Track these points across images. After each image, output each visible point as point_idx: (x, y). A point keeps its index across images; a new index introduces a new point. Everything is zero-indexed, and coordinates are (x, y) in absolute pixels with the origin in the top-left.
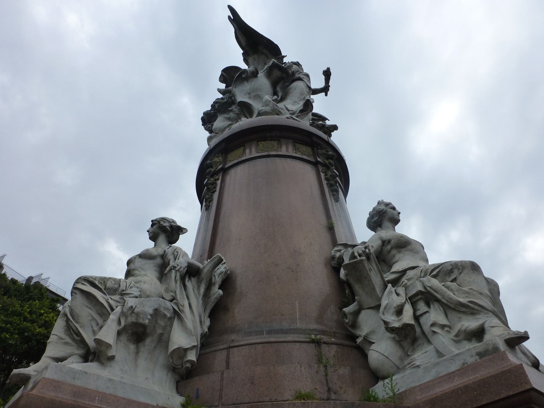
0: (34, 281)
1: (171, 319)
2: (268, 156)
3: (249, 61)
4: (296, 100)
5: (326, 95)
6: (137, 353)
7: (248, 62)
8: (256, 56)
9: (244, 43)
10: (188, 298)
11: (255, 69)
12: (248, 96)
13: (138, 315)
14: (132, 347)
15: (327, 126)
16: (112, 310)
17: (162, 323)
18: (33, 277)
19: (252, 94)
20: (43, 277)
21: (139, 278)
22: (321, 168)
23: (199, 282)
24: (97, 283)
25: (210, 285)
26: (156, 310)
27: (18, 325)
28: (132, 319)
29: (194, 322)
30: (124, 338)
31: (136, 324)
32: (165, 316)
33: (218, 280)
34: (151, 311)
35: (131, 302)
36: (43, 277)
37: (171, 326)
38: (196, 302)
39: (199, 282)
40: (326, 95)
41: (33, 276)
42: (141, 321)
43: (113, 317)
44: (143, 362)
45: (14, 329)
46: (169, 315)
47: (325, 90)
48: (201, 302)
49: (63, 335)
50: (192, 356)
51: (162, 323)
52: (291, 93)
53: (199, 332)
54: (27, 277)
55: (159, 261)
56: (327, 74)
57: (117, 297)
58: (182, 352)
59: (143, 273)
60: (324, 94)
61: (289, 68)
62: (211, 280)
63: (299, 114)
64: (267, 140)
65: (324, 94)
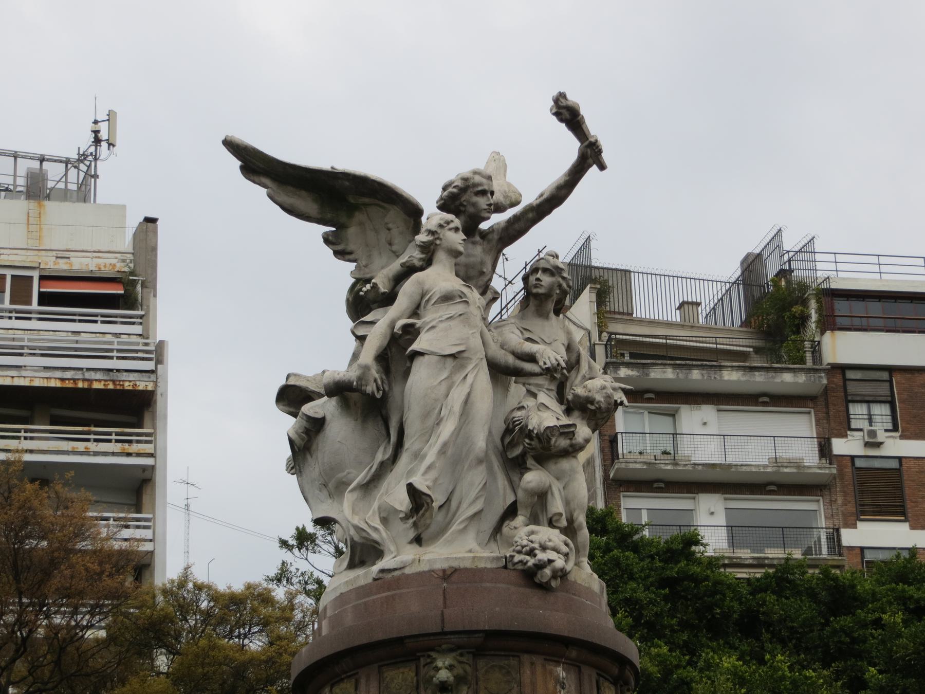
0: (772, 269)
3: (351, 247)
4: (416, 447)
5: (602, 167)
7: (350, 253)
8: (359, 216)
9: (312, 207)
11: (307, 421)
12: (325, 492)
15: (535, 432)
18: (759, 255)
19: (330, 485)
20: (790, 243)
36: (790, 243)
40: (602, 167)
41: (757, 251)
52: (405, 421)
54: (733, 271)
60: (594, 168)
61: (363, 383)
64: (342, 680)
65: (594, 168)
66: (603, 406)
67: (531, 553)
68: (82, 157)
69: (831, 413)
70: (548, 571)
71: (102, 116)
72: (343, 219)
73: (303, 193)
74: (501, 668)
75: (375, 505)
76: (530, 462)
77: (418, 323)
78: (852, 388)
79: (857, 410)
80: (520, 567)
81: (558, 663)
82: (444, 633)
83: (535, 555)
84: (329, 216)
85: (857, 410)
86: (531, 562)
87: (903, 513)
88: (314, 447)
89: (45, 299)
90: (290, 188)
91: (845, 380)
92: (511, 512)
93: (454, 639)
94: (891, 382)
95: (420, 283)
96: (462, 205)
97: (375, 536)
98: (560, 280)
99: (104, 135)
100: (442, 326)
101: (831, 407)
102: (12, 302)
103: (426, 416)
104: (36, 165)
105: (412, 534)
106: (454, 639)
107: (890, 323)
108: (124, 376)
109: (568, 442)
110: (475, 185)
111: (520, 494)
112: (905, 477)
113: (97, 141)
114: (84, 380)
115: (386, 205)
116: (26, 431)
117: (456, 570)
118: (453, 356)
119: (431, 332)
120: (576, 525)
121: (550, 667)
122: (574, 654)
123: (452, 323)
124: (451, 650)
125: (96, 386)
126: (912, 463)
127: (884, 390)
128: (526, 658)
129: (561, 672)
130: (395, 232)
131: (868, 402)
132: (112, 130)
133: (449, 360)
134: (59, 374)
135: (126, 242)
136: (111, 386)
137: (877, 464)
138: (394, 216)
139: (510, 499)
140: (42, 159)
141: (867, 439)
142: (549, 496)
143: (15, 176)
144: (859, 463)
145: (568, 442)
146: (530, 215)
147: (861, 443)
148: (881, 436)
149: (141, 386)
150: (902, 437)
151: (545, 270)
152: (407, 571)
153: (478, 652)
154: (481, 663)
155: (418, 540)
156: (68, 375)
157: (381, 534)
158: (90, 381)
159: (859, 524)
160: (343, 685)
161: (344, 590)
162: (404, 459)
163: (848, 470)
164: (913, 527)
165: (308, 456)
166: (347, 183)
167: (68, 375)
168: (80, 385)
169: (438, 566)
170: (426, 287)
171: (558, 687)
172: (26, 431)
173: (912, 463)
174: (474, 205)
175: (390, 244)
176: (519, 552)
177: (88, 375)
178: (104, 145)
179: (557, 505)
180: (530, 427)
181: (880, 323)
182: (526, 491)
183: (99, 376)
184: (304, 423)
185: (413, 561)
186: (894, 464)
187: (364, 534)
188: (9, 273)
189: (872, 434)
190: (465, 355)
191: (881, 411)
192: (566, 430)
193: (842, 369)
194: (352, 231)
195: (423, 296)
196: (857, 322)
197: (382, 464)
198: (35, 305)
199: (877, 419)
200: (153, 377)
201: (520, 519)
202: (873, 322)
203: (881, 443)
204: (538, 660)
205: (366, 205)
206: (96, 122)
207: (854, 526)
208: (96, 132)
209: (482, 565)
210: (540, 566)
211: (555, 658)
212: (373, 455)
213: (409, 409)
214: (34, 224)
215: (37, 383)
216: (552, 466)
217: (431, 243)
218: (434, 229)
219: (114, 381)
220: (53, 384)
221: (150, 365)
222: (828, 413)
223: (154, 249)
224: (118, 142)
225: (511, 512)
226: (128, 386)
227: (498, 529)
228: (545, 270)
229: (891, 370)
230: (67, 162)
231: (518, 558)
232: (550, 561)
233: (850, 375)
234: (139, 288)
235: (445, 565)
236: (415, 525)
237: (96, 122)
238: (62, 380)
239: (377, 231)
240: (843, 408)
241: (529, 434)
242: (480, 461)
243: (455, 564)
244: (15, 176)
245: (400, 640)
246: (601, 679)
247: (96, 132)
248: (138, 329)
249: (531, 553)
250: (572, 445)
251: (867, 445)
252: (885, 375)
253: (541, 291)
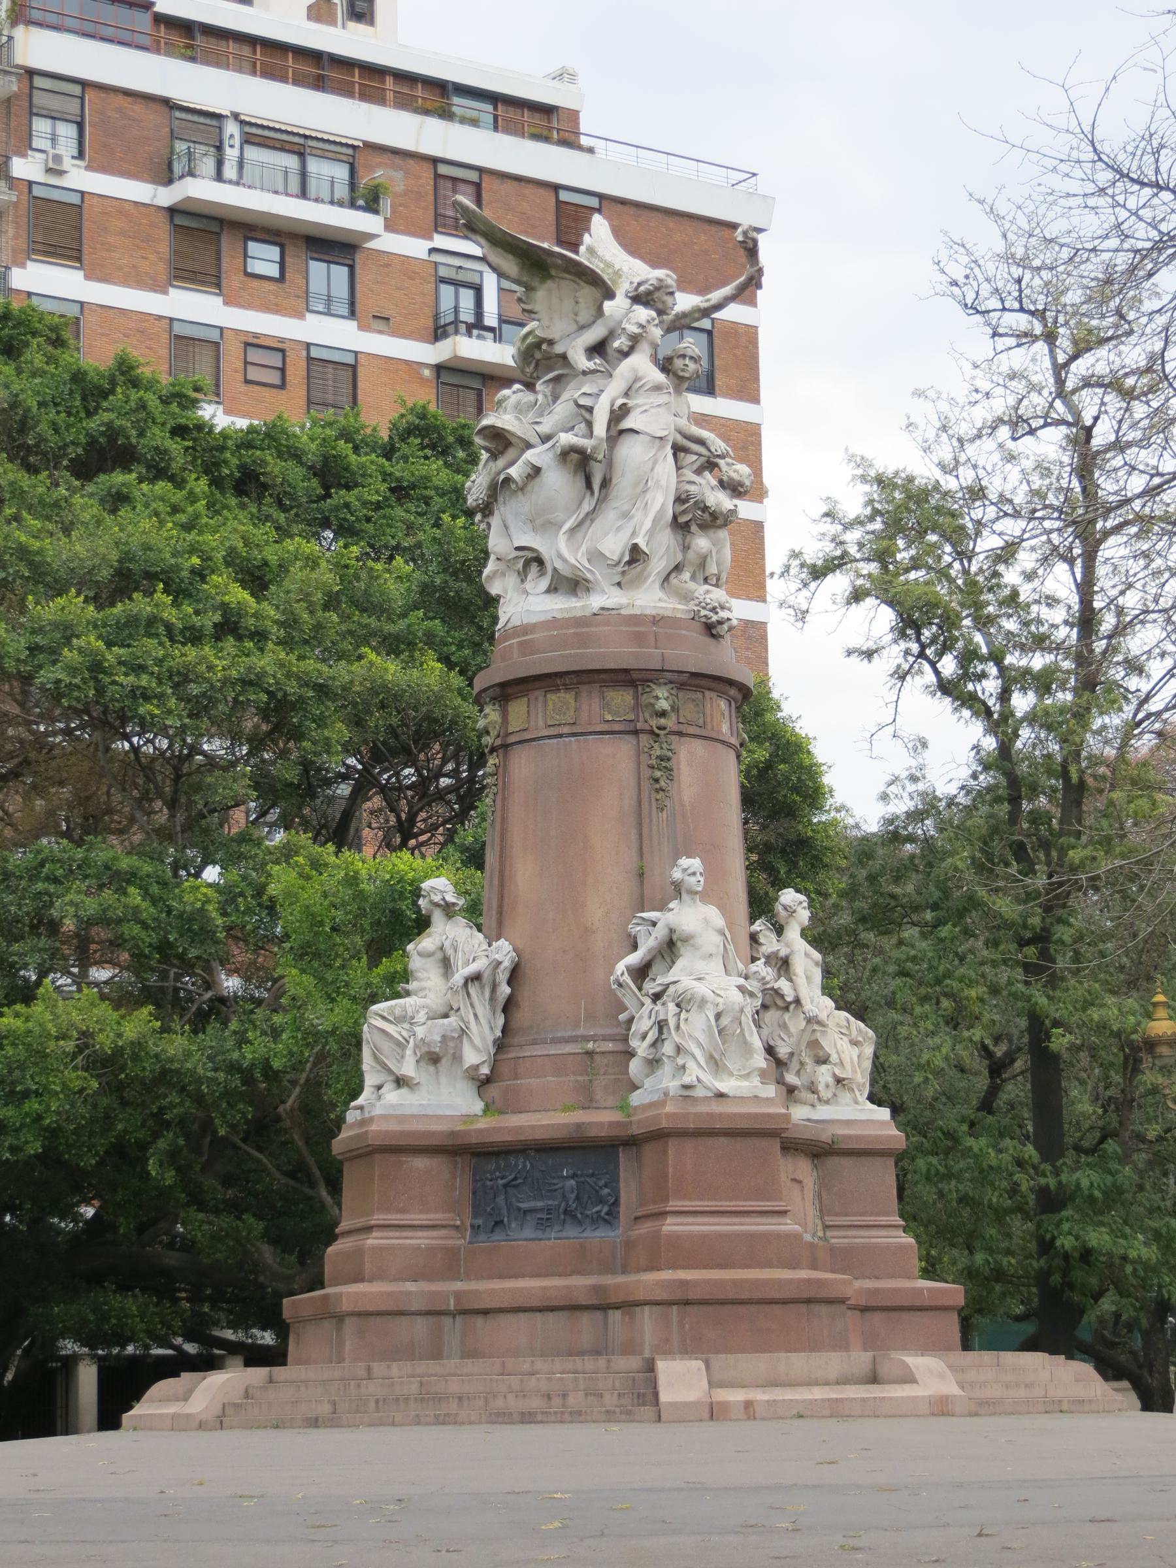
1: (460, 1038)
2: (561, 736)
4: (625, 508)
6: (437, 1072)
8: (550, 284)
10: (472, 1006)
13: (428, 1044)
14: (432, 1068)
16: (408, 1042)
17: (451, 1044)
21: (424, 984)
22: (644, 739)
23: (482, 987)
24: (385, 1014)
25: (494, 987)
26: (444, 1037)
27: (160, 662)
28: (425, 1049)
29: (481, 1033)
30: (422, 1064)
31: (429, 1053)
32: (453, 1038)
33: (503, 976)
34: (438, 1038)
35: (420, 1032)
37: (462, 1042)
38: (482, 1009)
39: (482, 987)
42: (433, 1050)
43: (409, 1052)
44: (444, 1080)
45: (160, 682)
46: (456, 1035)
48: (488, 1007)
49: (374, 1064)
50: (485, 1070)
51: (451, 1044)
53: (490, 1039)
55: (439, 955)
57: (406, 1026)
58: (476, 1068)
59: (426, 975)
62: (494, 981)
63: (626, 568)
67: (714, 610)
69: (12, 125)
70: (725, 627)
72: (535, 282)
73: (510, 257)
74: (693, 700)
75: (584, 548)
76: (694, 528)
77: (631, 403)
78: (39, 99)
79: (41, 126)
80: (703, 620)
82: (663, 671)
83: (717, 613)
84: (525, 279)
85: (41, 126)
86: (715, 618)
87: (79, 259)
88: (529, 488)
90: (500, 250)
91: (32, 87)
92: (678, 568)
93: (669, 675)
94: (82, 98)
95: (635, 370)
96: (653, 300)
97: (589, 576)
100: (653, 411)
101: (13, 117)
103: (636, 484)
105: (617, 579)
106: (669, 675)
107: (90, 27)
110: (667, 287)
111: (691, 555)
112: (85, 216)
115: (583, 284)
117: (663, 618)
118: (661, 438)
119: (644, 415)
123: (660, 409)
124: (665, 684)
126: (96, 200)
127: (73, 107)
128: (707, 693)
129: (723, 705)
130: (582, 305)
131: (53, 118)
133: (657, 441)
137: (56, 195)
138: (587, 293)
139: (679, 557)
141: (51, 165)
142: (709, 559)
144: (37, 191)
146: (697, 315)
147: (42, 167)
148: (68, 163)
150: (88, 168)
151: (691, 358)
152: (623, 612)
153: (681, 686)
154: (681, 694)
155: (619, 584)
157: (596, 574)
159: (29, 263)
160: (562, 694)
161: (559, 616)
162: (609, 517)
163: (25, 197)
164: (87, 277)
165: (520, 494)
166: (560, 262)
169: (648, 612)
170: (640, 374)
173: (96, 200)
174: (664, 303)
175: (576, 315)
176: (704, 608)
179: (712, 569)
180: (708, 504)
181: (73, 23)
182: (698, 554)
184: (529, 470)
185: (628, 605)
186: (75, 199)
187: (579, 573)
189: (58, 159)
191: (67, 131)
193: (31, 73)
194: (540, 294)
195: (636, 380)
196: (52, 19)
197: (588, 514)
199: (61, 141)
201: (686, 575)
202: (69, 22)
203: (66, 172)
204: (713, 695)
205: (562, 278)
207: (23, 265)
209: (679, 616)
210: (720, 623)
211: (721, 694)
212: (580, 504)
213: (622, 475)
216: (711, 532)
217: (640, 335)
218: (644, 323)
222: (8, 124)
225: (678, 568)
227: (667, 579)
228: (691, 358)
229: (84, 84)
231: (703, 613)
232: (729, 619)
233: (39, 82)
235: (653, 612)
236: (623, 573)
239: (561, 299)
240: (25, 122)
241: (705, 509)
243: (661, 612)
245: (626, 671)
249: (714, 610)
251: (49, 171)
252: (76, 90)
253: (686, 375)
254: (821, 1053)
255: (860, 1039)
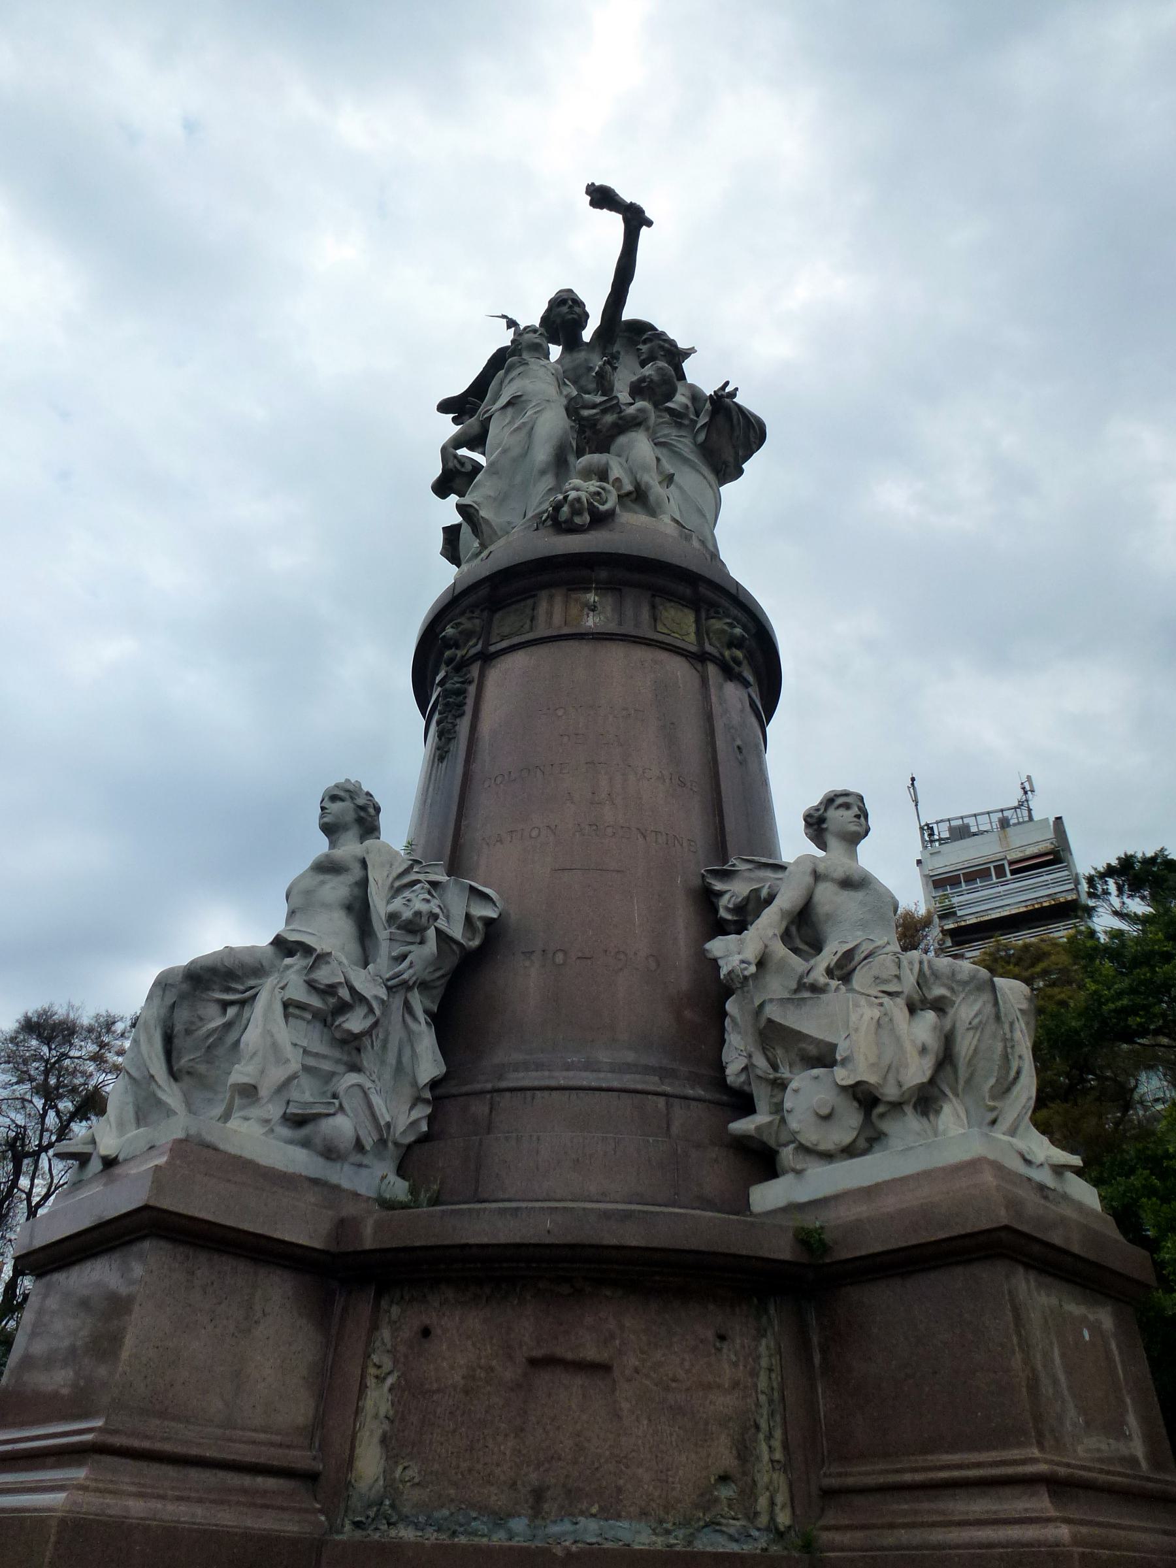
5: (649, 223)
40: (649, 223)
47: (635, 219)
56: (602, 197)
60: (644, 229)
66: (656, 378)
68: (1021, 805)
71: (1024, 779)
81: (588, 590)
89: (1013, 872)
98: (661, 342)
99: (1028, 788)
102: (997, 878)
104: (1000, 815)
108: (1058, 895)
109: (615, 416)
113: (1026, 793)
114: (1037, 903)
116: (1014, 937)
120: (643, 487)
121: (574, 596)
122: (603, 574)
125: (1045, 904)
128: (544, 594)
132: (1031, 785)
134: (1024, 904)
135: (1050, 834)
136: (1053, 903)
140: (1002, 811)
143: (991, 823)
145: (615, 416)
149: (1069, 898)
156: (1029, 903)
158: (1041, 903)
167: (1029, 903)
168: (1036, 906)
171: (586, 610)
172: (1014, 937)
177: (1039, 900)
178: (1029, 793)
183: (1045, 899)
188: (991, 866)
190: (524, 398)
192: (608, 405)
198: (1009, 876)
200: (1075, 892)
206: (1022, 784)
208: (1024, 788)
214: (1003, 839)
215: (1013, 912)
216: (613, 448)
219: (1053, 900)
220: (1022, 910)
221: (1072, 886)
223: (1065, 832)
224: (1036, 788)
226: (1062, 900)
230: (1015, 808)
234: (1061, 853)
237: (1022, 784)
238: (1026, 906)
242: (543, 472)
244: (991, 823)
246: (658, 600)
247: (1024, 788)
248: (1066, 873)
250: (620, 418)
254: (812, 1050)
255: (938, 991)
